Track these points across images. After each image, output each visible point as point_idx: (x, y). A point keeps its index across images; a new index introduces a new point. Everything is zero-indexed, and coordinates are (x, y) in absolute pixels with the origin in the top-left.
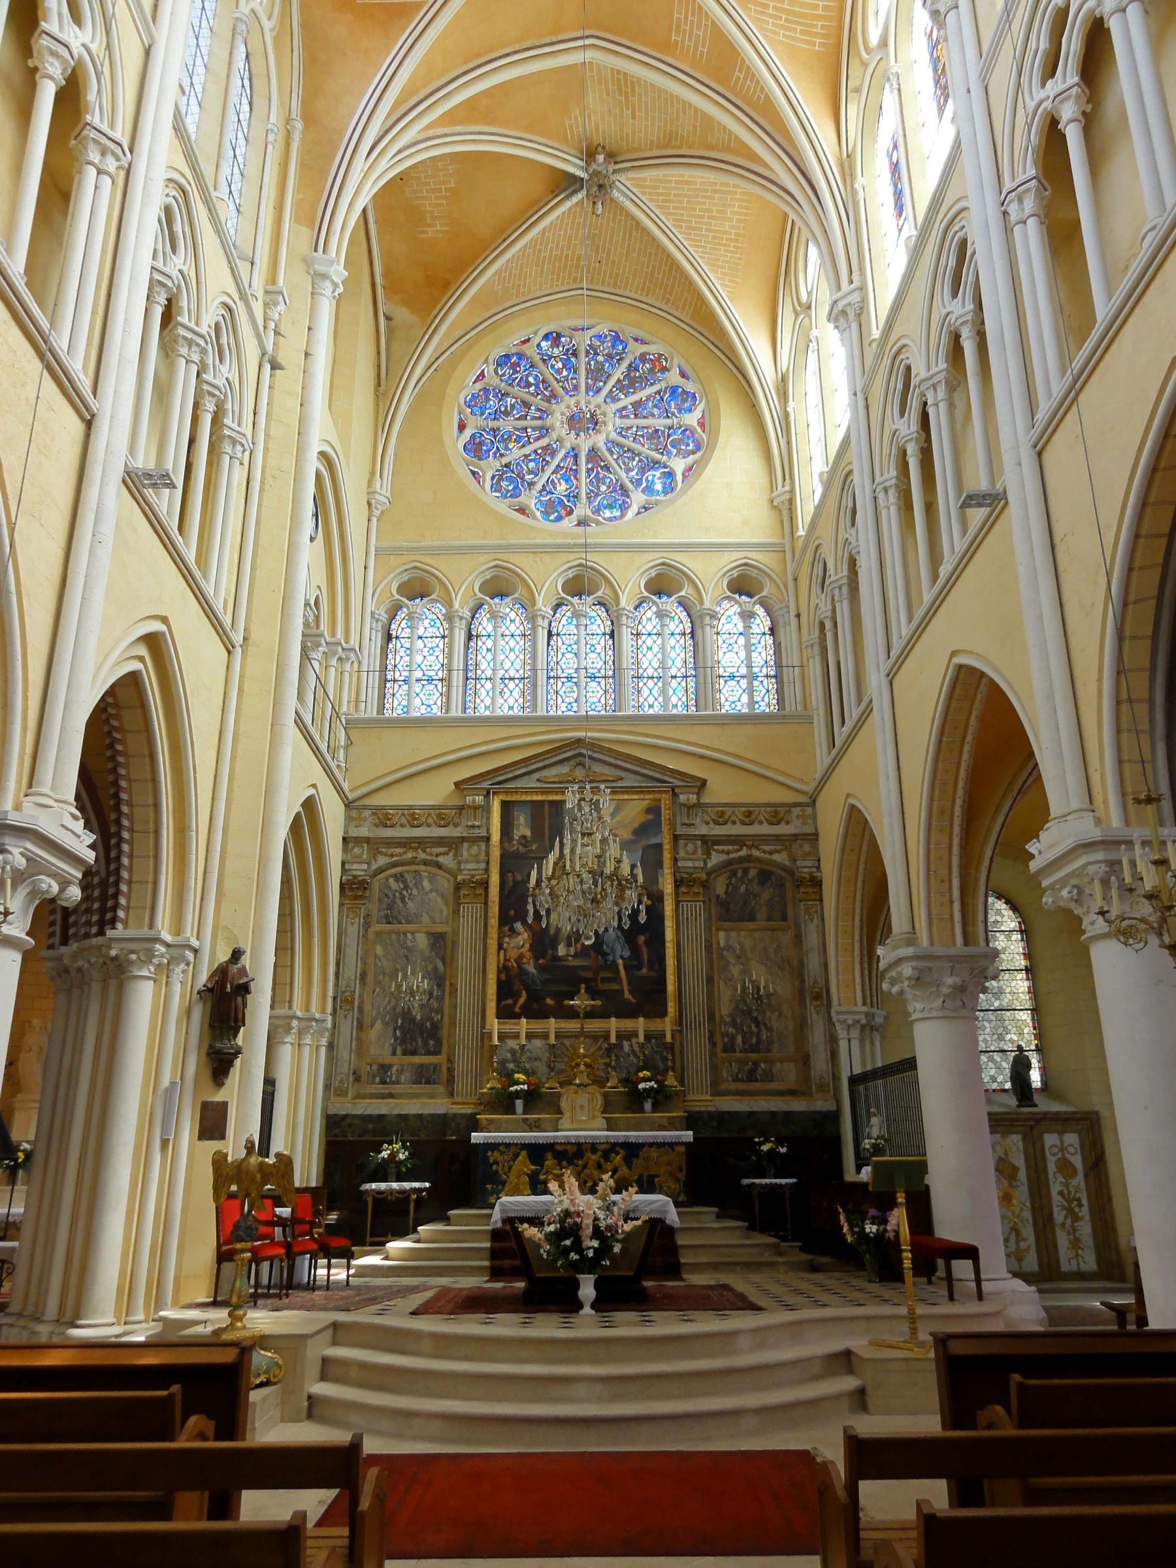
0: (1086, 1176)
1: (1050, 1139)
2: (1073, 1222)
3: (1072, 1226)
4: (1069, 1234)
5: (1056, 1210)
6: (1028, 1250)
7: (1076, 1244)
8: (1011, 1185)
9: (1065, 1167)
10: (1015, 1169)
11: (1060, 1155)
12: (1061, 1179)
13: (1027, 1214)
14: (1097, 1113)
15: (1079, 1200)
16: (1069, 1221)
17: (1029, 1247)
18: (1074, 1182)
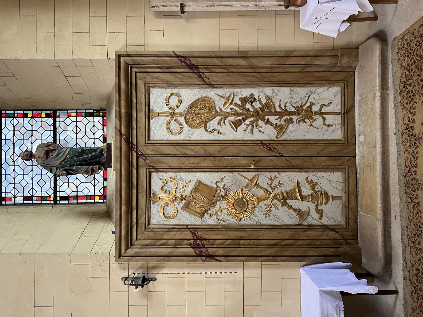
0: (211, 85)
1: (159, 131)
2: (276, 113)
3: (281, 115)
4: (290, 121)
5: (257, 136)
6: (313, 185)
7: (306, 113)
8: (223, 198)
9: (200, 112)
10: (199, 186)
11: (182, 119)
12: (213, 124)
13: (264, 178)
14: (119, 56)
15: (244, 100)
16: (272, 119)
17: (311, 182)
18: (219, 104)
